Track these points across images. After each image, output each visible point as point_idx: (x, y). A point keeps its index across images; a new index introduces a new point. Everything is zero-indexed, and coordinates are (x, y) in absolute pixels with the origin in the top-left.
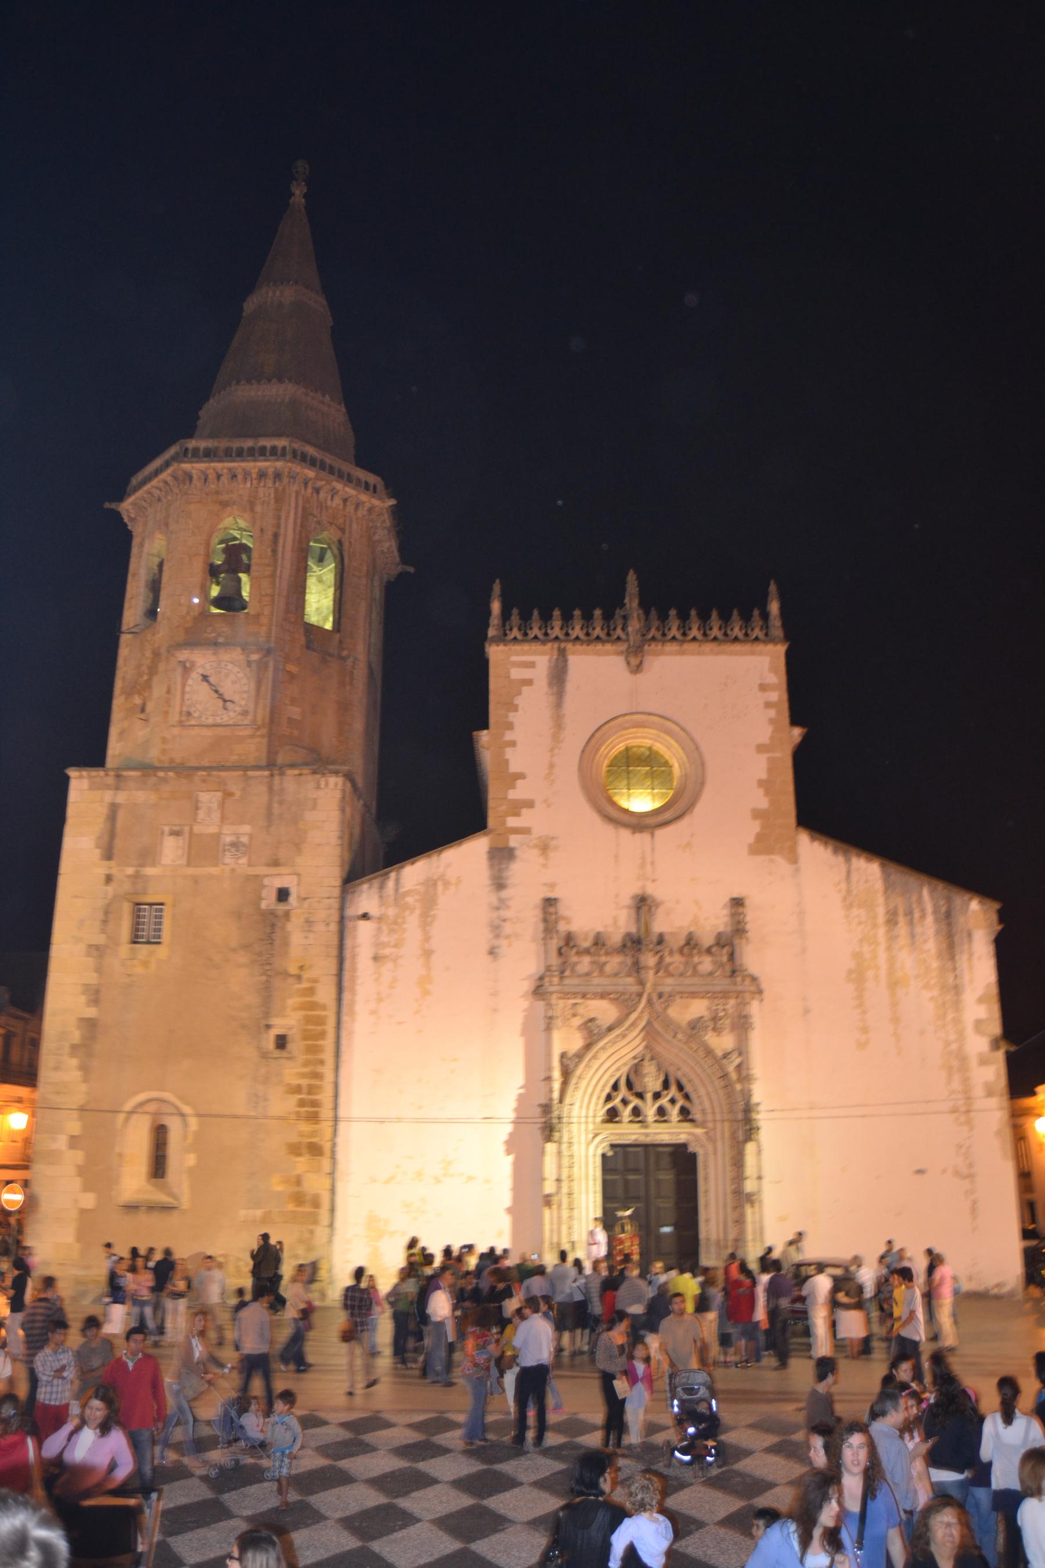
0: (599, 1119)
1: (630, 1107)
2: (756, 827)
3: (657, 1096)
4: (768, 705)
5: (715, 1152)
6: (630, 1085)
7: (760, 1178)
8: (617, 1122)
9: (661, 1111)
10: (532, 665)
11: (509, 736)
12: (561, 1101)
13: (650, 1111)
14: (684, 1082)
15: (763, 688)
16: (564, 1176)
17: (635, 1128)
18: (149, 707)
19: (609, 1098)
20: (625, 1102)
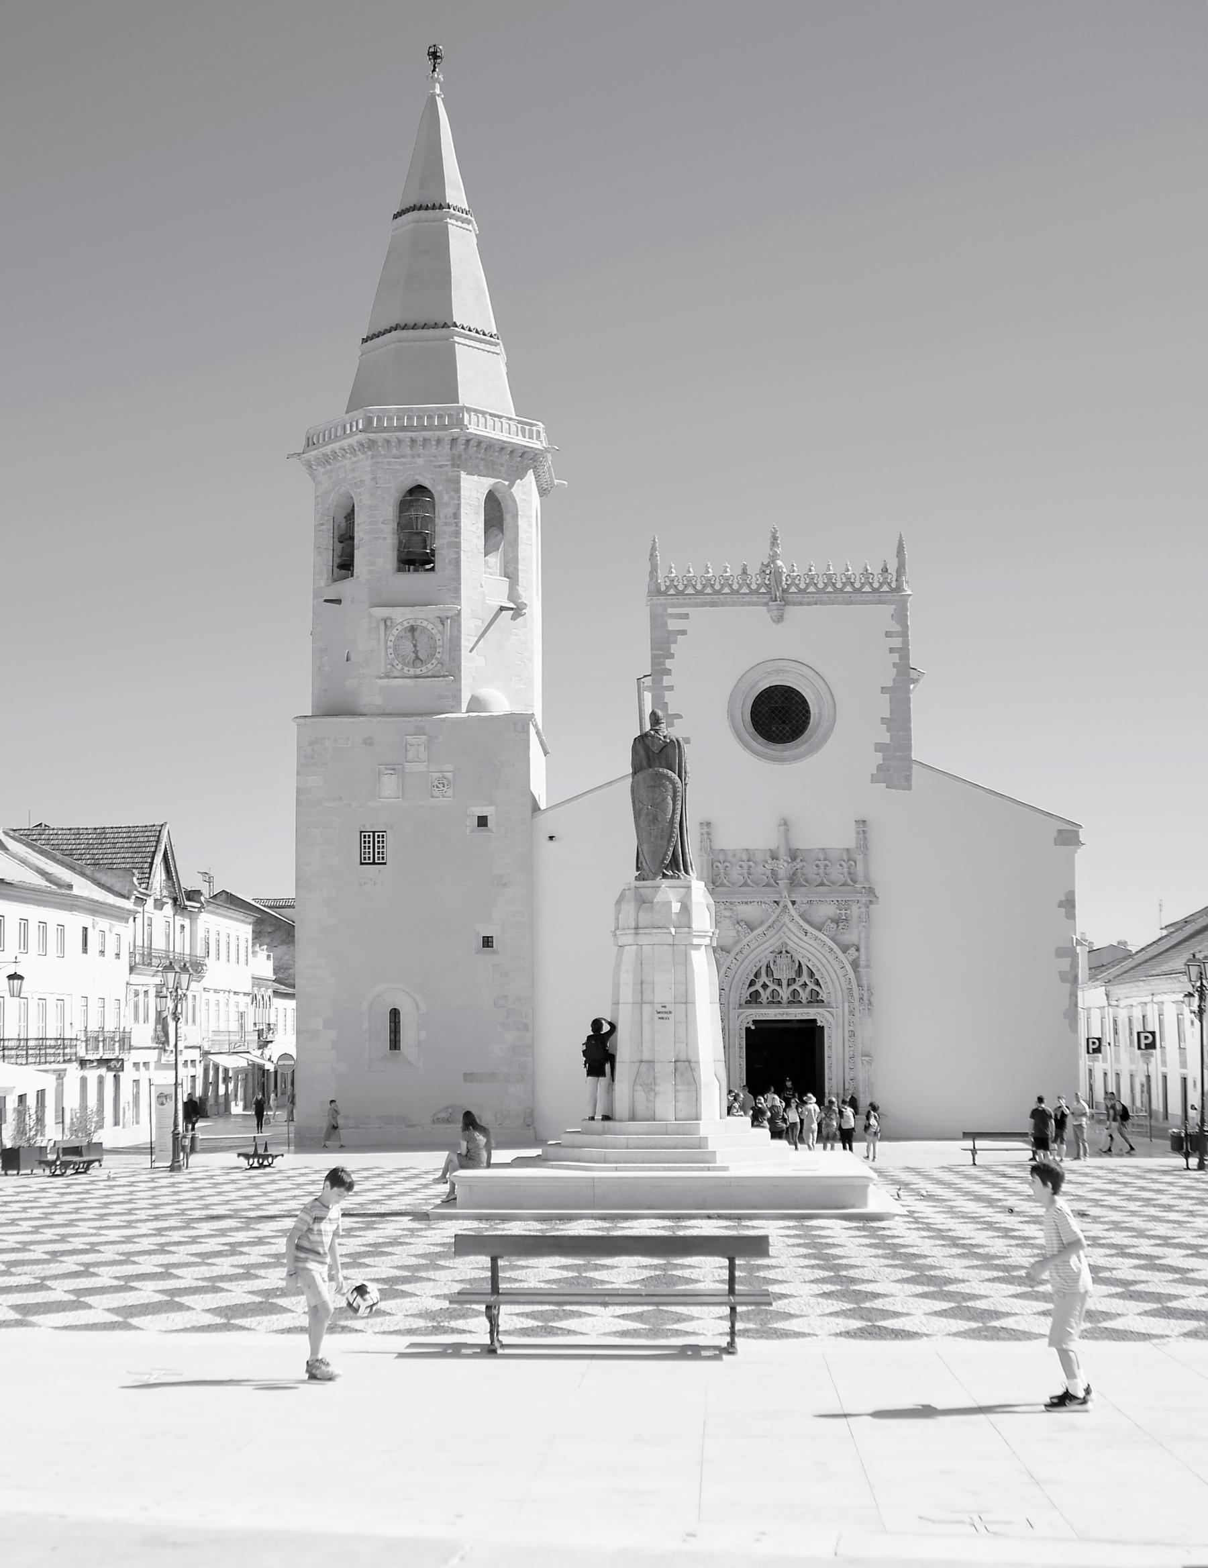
0: (743, 1001)
1: (769, 990)
2: (878, 758)
3: (791, 982)
4: (891, 650)
10: (686, 616)
11: (667, 680)
15: (888, 634)
18: (353, 658)
19: (752, 983)
20: (765, 986)
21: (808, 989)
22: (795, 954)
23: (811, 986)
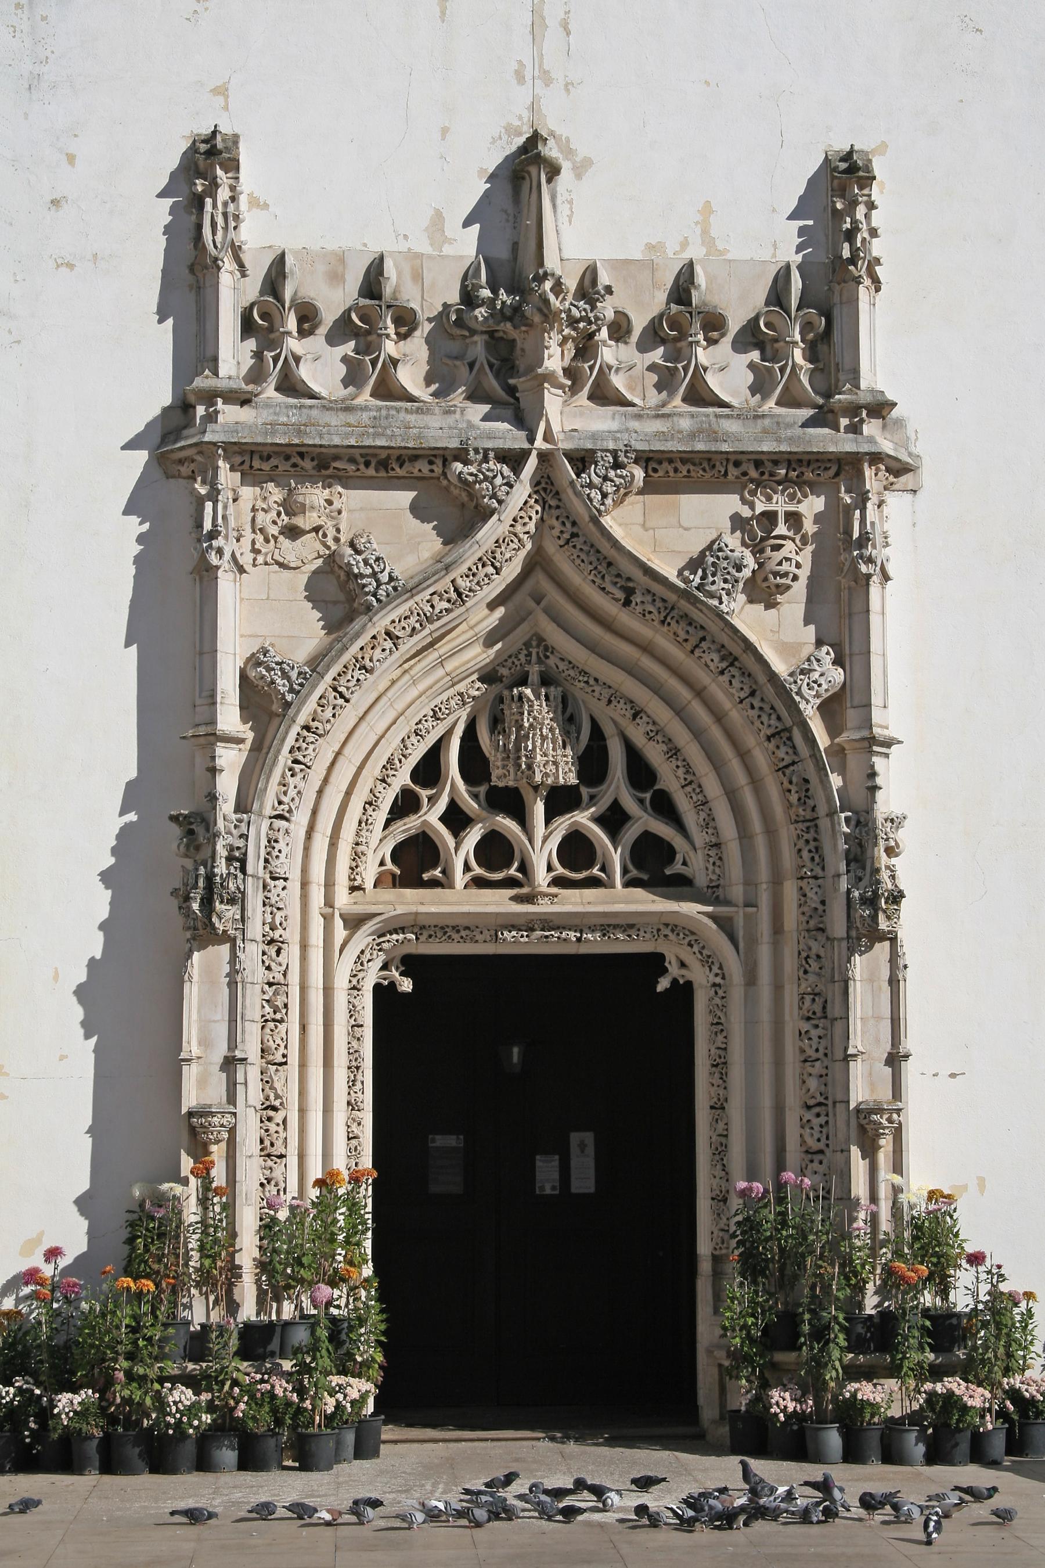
0: (369, 874)
1: (474, 836)
5: (751, 979)
6: (474, 765)
7: (895, 1060)
8: (434, 883)
9: (576, 851)
12: (242, 806)
13: (542, 845)
14: (654, 754)
16: (250, 1048)
17: (497, 902)
19: (406, 805)
20: (456, 819)
21: (631, 833)
22: (578, 689)
23: (643, 821)
